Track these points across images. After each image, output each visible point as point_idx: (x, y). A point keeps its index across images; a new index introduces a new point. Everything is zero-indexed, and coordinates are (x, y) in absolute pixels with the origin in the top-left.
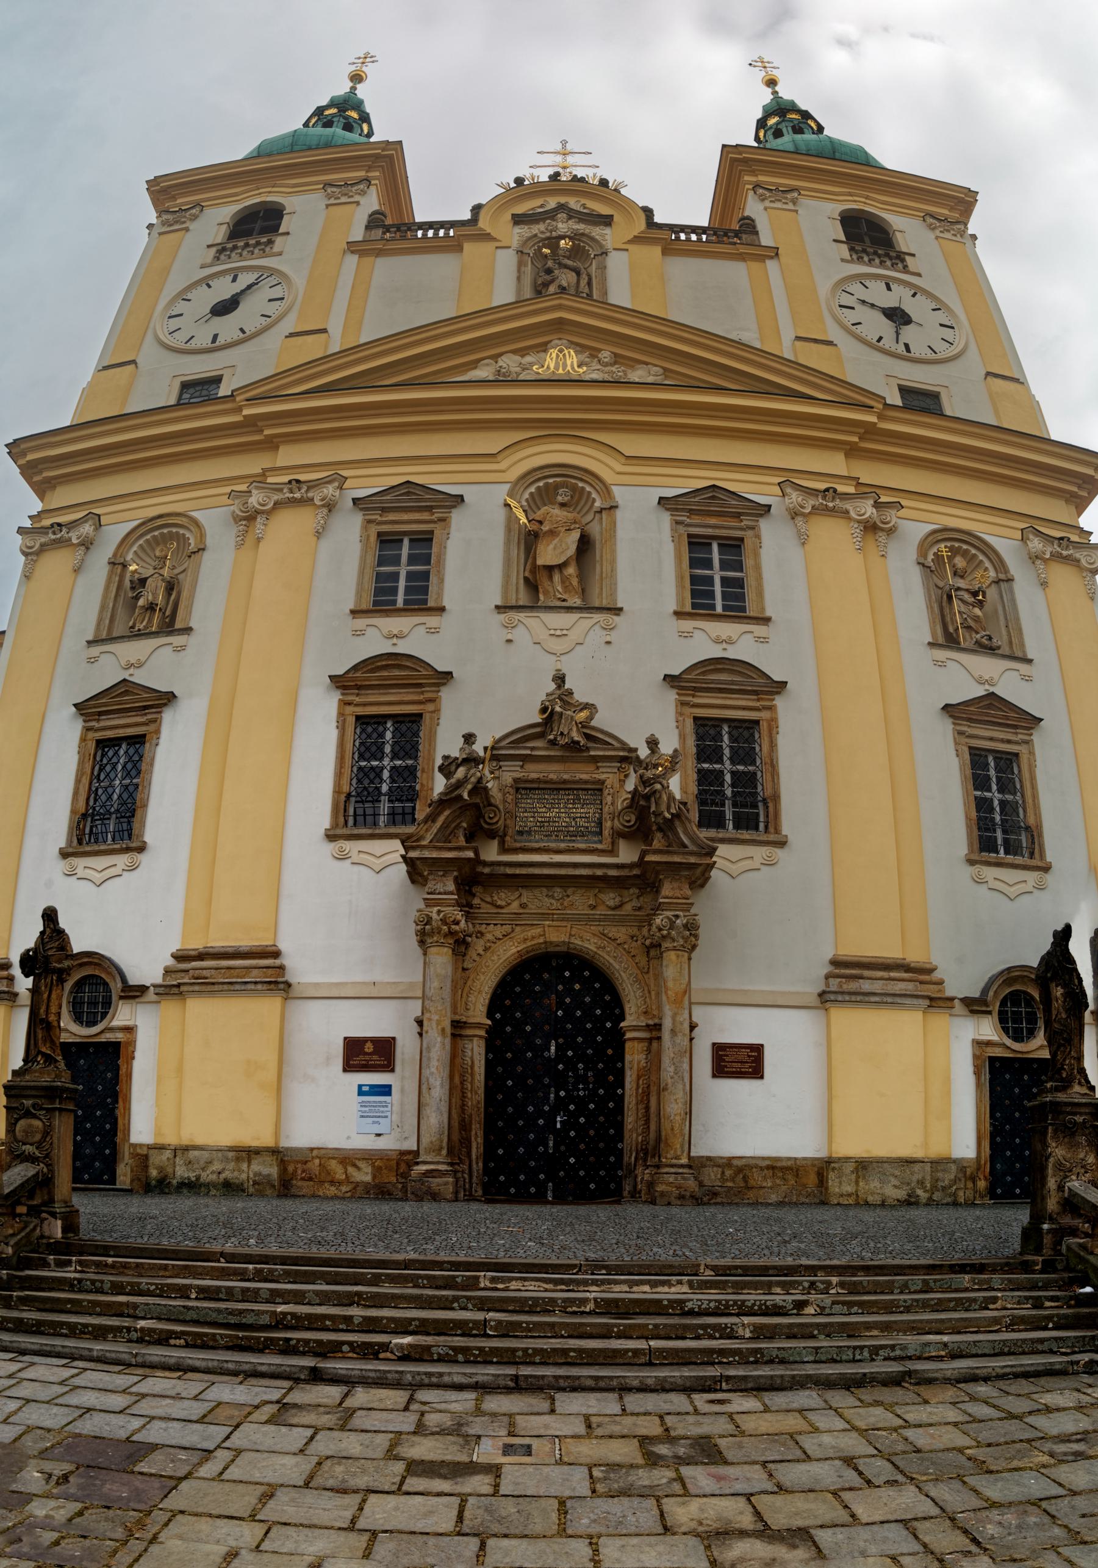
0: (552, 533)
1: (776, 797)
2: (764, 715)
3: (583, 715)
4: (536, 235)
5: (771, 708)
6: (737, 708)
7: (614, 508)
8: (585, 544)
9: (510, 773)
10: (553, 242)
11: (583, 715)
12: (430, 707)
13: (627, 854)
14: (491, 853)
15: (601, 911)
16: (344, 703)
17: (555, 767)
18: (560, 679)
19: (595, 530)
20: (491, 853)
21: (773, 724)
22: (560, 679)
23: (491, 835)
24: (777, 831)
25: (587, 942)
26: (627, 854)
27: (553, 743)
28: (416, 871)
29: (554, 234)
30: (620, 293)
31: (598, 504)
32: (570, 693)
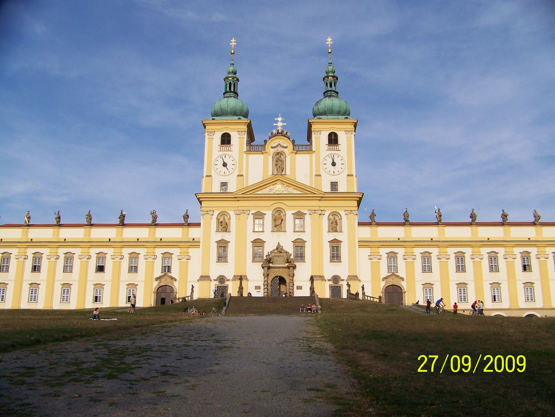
0: (278, 220)
1: (305, 256)
2: (304, 245)
3: (281, 247)
4: (275, 152)
5: (305, 244)
6: (300, 244)
7: (286, 215)
8: (282, 220)
9: (273, 254)
10: (278, 154)
11: (281, 247)
12: (263, 245)
13: (287, 265)
14: (271, 265)
15: (284, 271)
16: (252, 245)
17: (278, 254)
18: (279, 243)
19: (283, 217)
20: (271, 265)
21: (305, 246)
22: (279, 243)
23: (271, 263)
24: (305, 261)
25: (282, 275)
26: (287, 265)
27: (278, 251)
28: (263, 267)
29: (278, 152)
30: (288, 172)
31: (284, 214)
32: (280, 245)
